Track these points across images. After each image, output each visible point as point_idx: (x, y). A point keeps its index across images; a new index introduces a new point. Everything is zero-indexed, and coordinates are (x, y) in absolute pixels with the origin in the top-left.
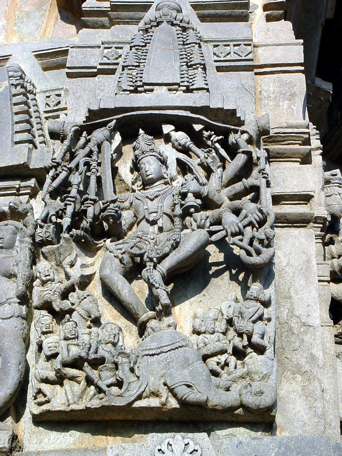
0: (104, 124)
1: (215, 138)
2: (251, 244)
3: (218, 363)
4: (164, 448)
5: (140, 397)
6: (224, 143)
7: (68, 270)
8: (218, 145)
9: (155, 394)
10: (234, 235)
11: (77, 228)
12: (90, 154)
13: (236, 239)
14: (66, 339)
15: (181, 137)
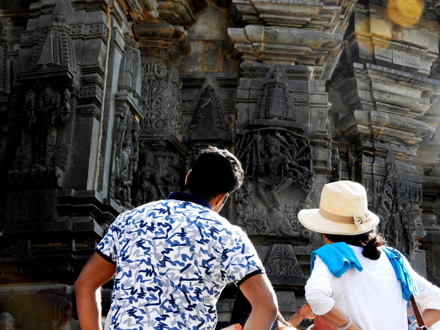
0: (256, 132)
1: (294, 139)
2: (306, 184)
3: (294, 223)
4: (279, 248)
5: (271, 233)
6: (297, 141)
7: (247, 189)
8: (295, 142)
9: (275, 232)
10: (301, 180)
11: (250, 175)
12: (252, 146)
13: (301, 182)
14: (247, 213)
15: (282, 138)
